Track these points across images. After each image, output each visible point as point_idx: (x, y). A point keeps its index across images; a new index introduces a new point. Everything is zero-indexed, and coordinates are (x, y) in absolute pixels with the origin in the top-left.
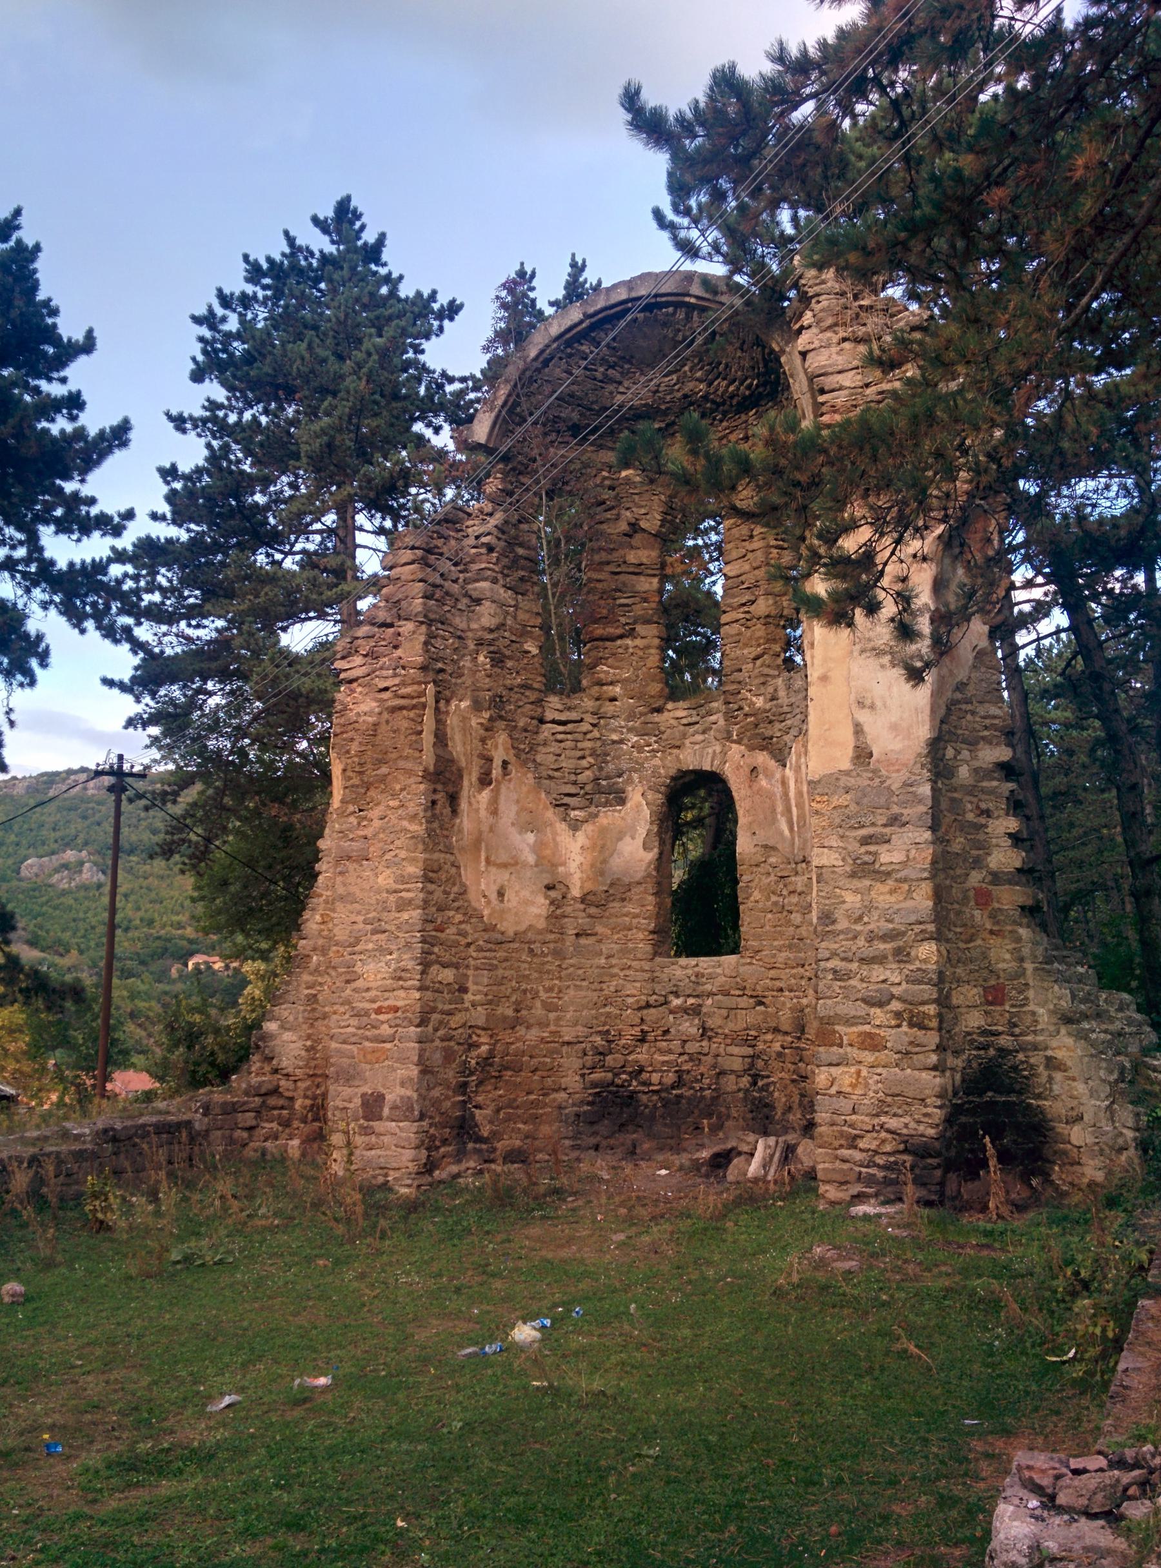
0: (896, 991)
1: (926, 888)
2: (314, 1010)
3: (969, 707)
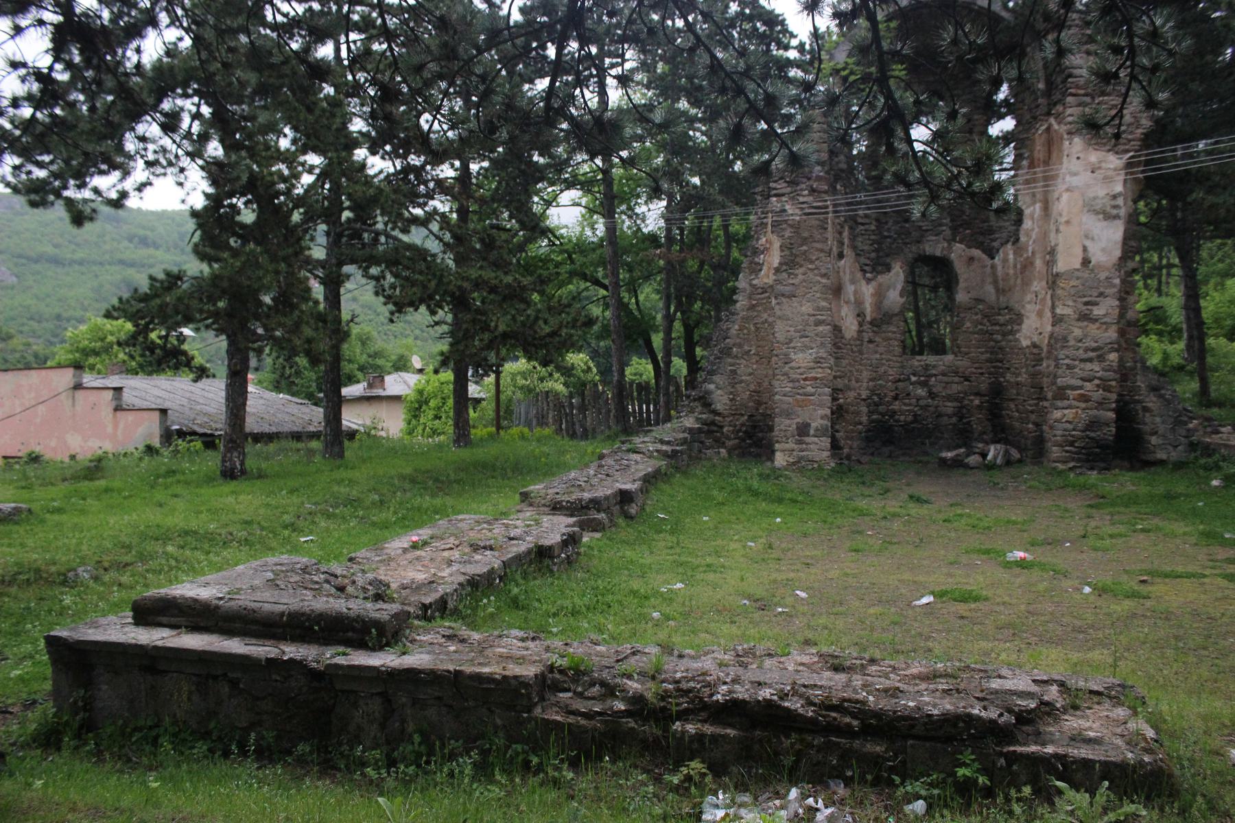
0: (1098, 375)
1: (1114, 327)
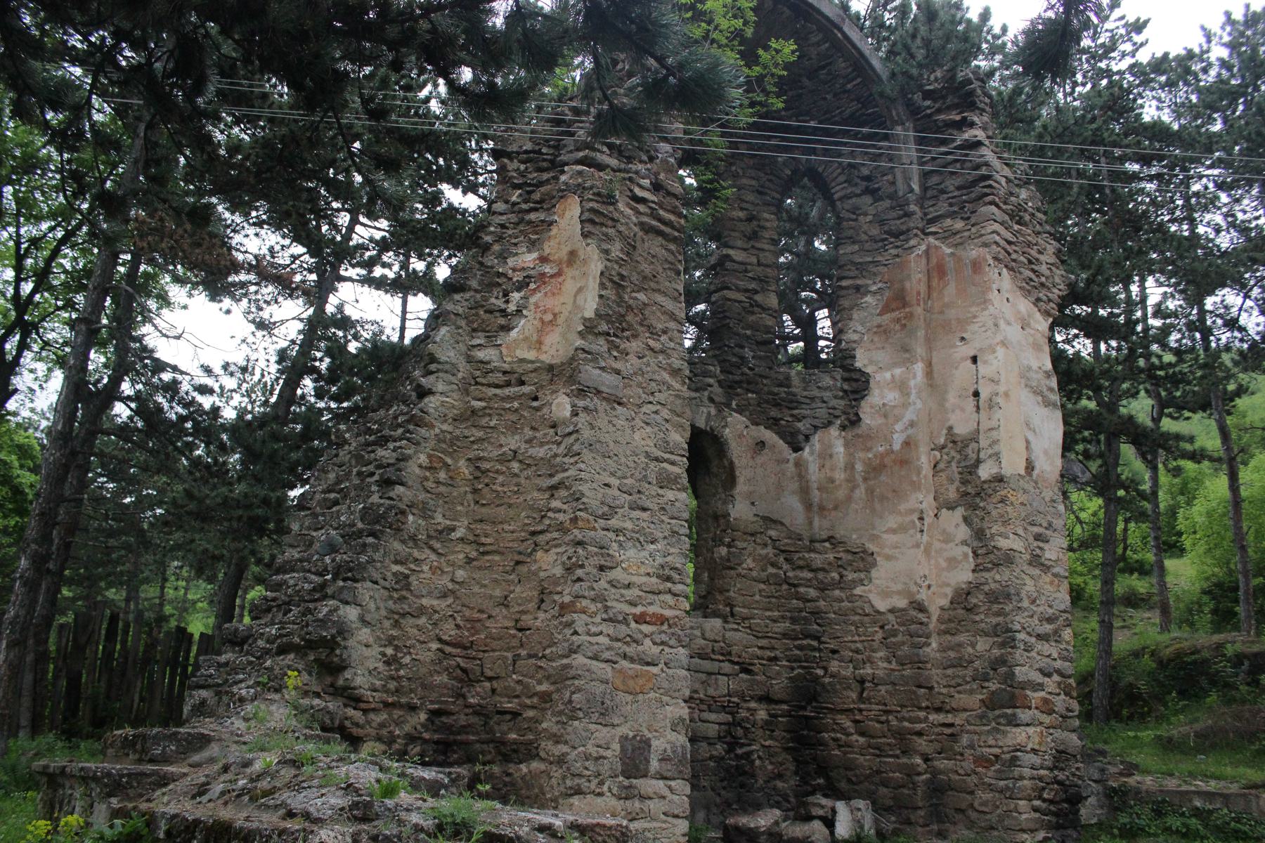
2: (402, 599)
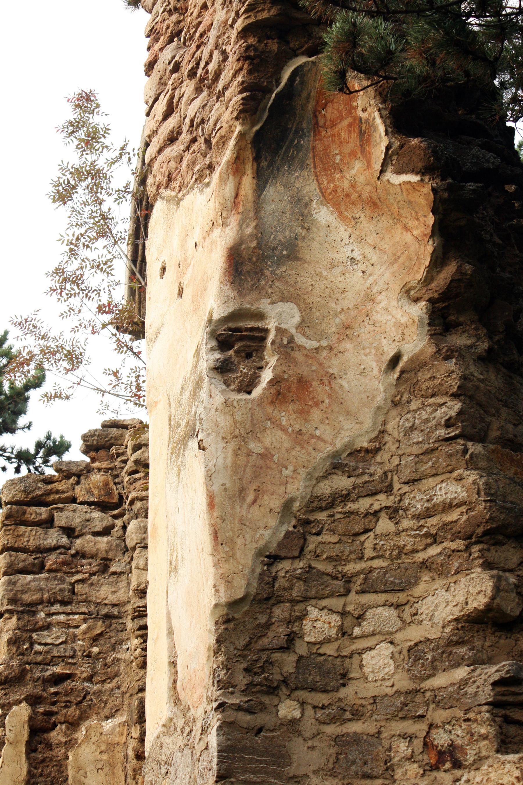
3: (383, 500)
